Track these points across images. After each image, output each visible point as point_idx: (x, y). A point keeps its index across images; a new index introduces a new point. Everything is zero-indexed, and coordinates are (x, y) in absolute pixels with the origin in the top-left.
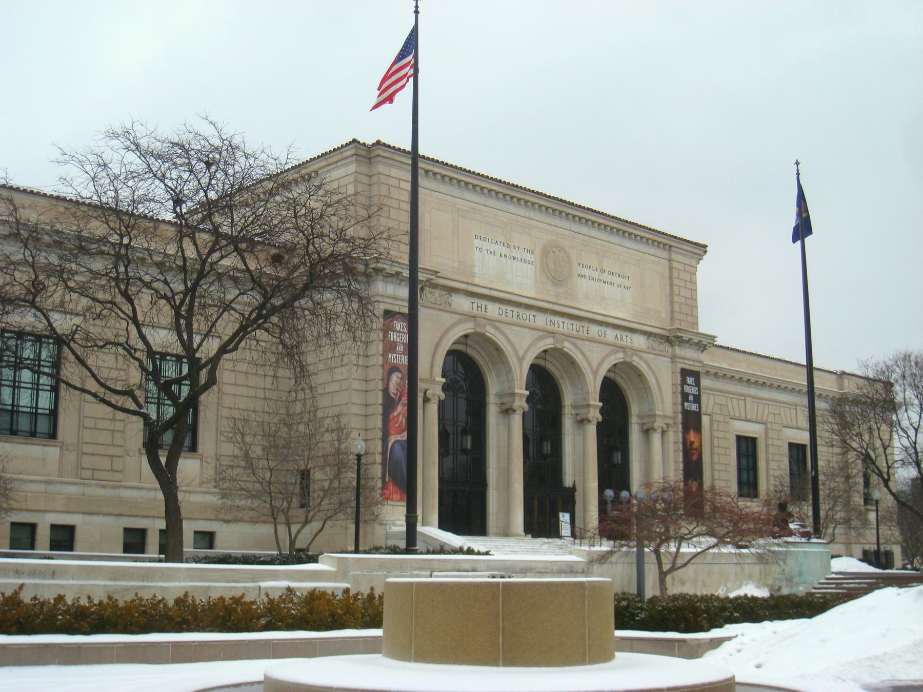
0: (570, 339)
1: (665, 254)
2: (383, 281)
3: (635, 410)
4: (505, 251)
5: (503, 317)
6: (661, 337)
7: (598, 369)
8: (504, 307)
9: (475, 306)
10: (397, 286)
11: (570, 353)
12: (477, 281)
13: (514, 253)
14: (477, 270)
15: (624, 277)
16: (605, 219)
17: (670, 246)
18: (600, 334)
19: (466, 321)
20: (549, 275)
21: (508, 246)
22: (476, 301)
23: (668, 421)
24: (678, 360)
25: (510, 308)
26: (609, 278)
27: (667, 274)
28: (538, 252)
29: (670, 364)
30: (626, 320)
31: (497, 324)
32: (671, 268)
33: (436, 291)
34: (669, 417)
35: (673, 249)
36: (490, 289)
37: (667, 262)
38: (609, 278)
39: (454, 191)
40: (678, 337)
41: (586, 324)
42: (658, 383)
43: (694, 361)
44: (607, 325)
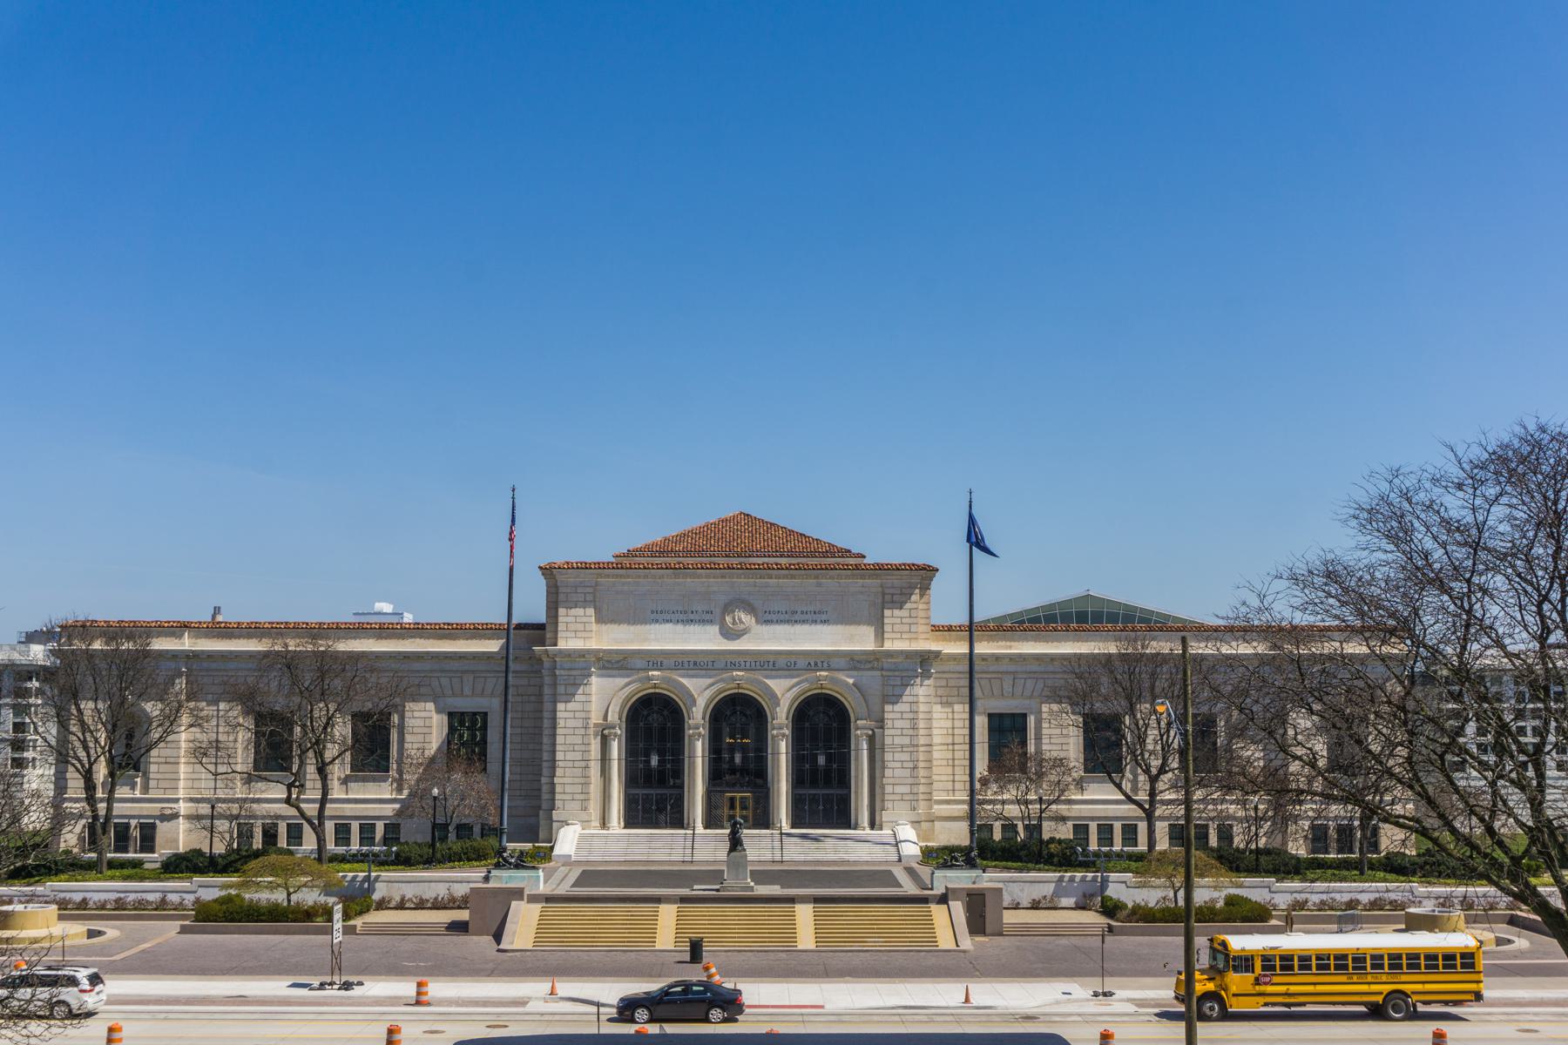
13: (692, 617)
15: (820, 612)
18: (789, 664)
21: (686, 612)
32: (884, 594)
37: (880, 589)
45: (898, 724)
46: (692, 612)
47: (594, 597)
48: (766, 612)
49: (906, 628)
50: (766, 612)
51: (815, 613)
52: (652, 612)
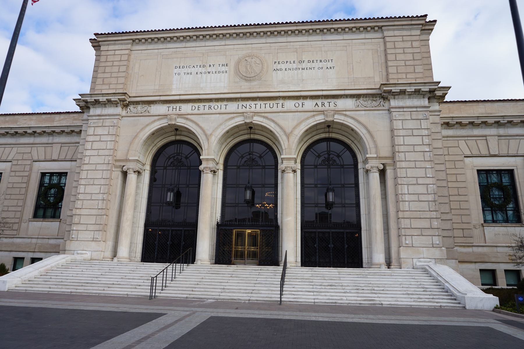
0: (263, 114)
1: (379, 35)
2: (94, 107)
3: (360, 159)
4: (203, 70)
5: (196, 111)
6: (373, 96)
7: (292, 132)
8: (196, 105)
9: (171, 109)
10: (104, 108)
11: (262, 124)
12: (173, 93)
13: (209, 69)
14: (174, 87)
16: (297, 26)
17: (380, 28)
19: (158, 120)
20: (241, 76)
21: (204, 66)
22: (172, 105)
23: (384, 161)
24: (392, 110)
25: (201, 105)
26: (309, 65)
27: (382, 48)
28: (232, 64)
29: (388, 115)
30: (323, 90)
31: (189, 117)
32: (385, 43)
33: (139, 106)
34: (386, 158)
35: (383, 28)
36: (180, 95)
38: (309, 65)
39: (161, 46)
40: (390, 92)
41: (281, 102)
42: (369, 132)
43: (417, 107)
44: (305, 97)
45: (411, 156)
46: (210, 66)
47: (128, 58)
48: (275, 62)
49: (411, 69)
50: (275, 62)
51: (321, 61)
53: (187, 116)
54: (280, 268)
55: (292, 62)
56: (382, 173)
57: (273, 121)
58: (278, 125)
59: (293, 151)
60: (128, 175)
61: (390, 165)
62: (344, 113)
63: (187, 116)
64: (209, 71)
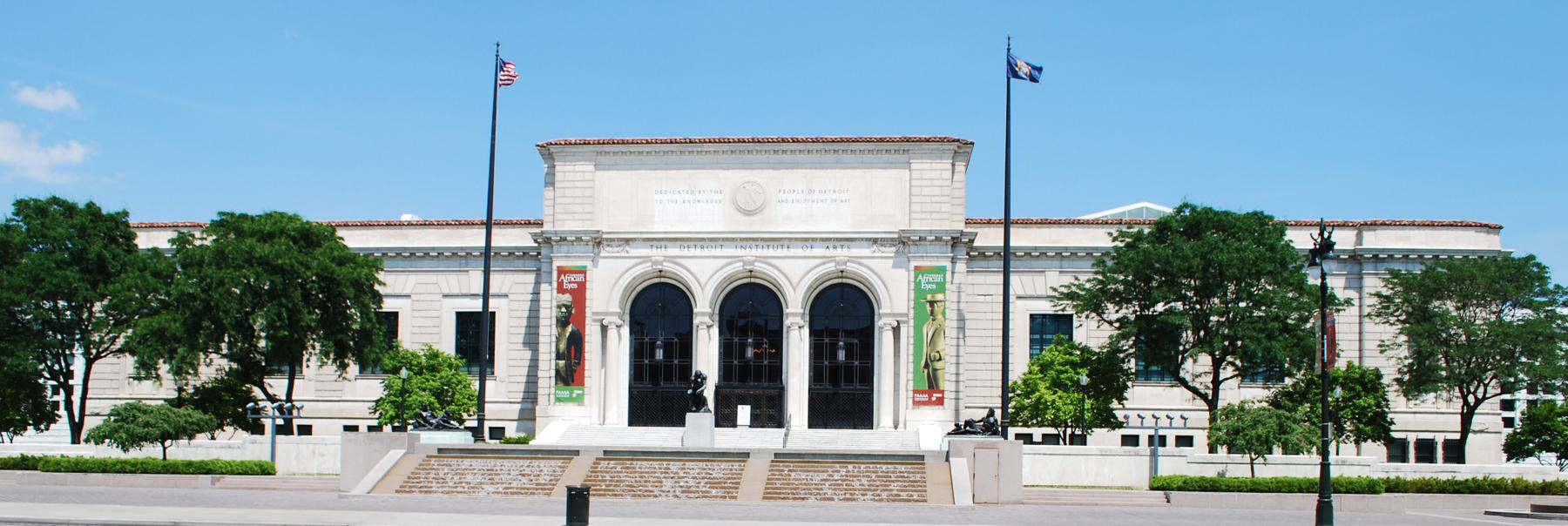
4: (692, 198)
15: (840, 191)
19: (641, 263)
21: (692, 192)
31: (679, 260)
38: (820, 196)
46: (700, 192)
48: (780, 191)
50: (780, 191)
51: (834, 191)
52: (656, 192)
53: (675, 260)
54: (783, 431)
55: (800, 192)
56: (896, 331)
57: (777, 269)
58: (783, 274)
59: (800, 304)
60: (609, 332)
61: (904, 322)
62: (858, 260)
63: (675, 260)
64: (699, 199)
